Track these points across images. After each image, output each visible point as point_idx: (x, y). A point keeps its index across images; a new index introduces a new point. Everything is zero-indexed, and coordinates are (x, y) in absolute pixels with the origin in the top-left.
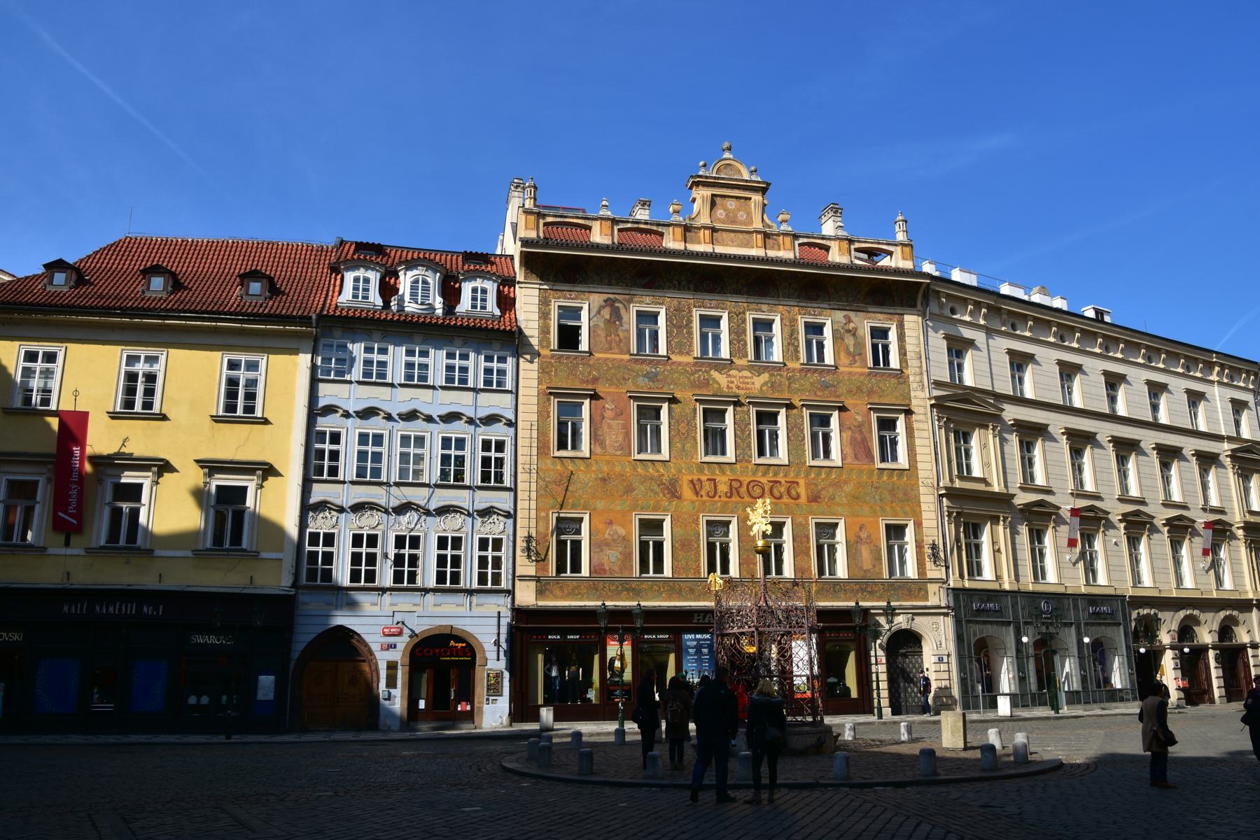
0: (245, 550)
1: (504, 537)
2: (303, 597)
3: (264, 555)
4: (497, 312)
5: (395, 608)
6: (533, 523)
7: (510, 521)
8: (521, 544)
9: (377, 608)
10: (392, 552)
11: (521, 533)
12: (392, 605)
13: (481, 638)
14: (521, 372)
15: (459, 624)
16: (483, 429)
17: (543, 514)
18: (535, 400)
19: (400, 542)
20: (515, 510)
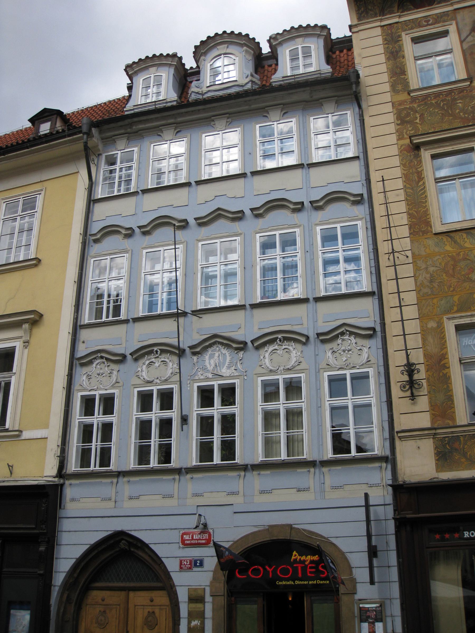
0: (7, 430)
1: (371, 371)
2: (71, 491)
3: (26, 435)
4: (327, 69)
5: (200, 501)
6: (414, 341)
7: (376, 343)
8: (398, 377)
9: (173, 502)
10: (195, 411)
11: (397, 360)
12: (196, 495)
13: (343, 545)
14: (370, 132)
15: (305, 522)
16: (320, 215)
17: (432, 324)
18: (396, 161)
19: (206, 397)
20: (383, 325)
